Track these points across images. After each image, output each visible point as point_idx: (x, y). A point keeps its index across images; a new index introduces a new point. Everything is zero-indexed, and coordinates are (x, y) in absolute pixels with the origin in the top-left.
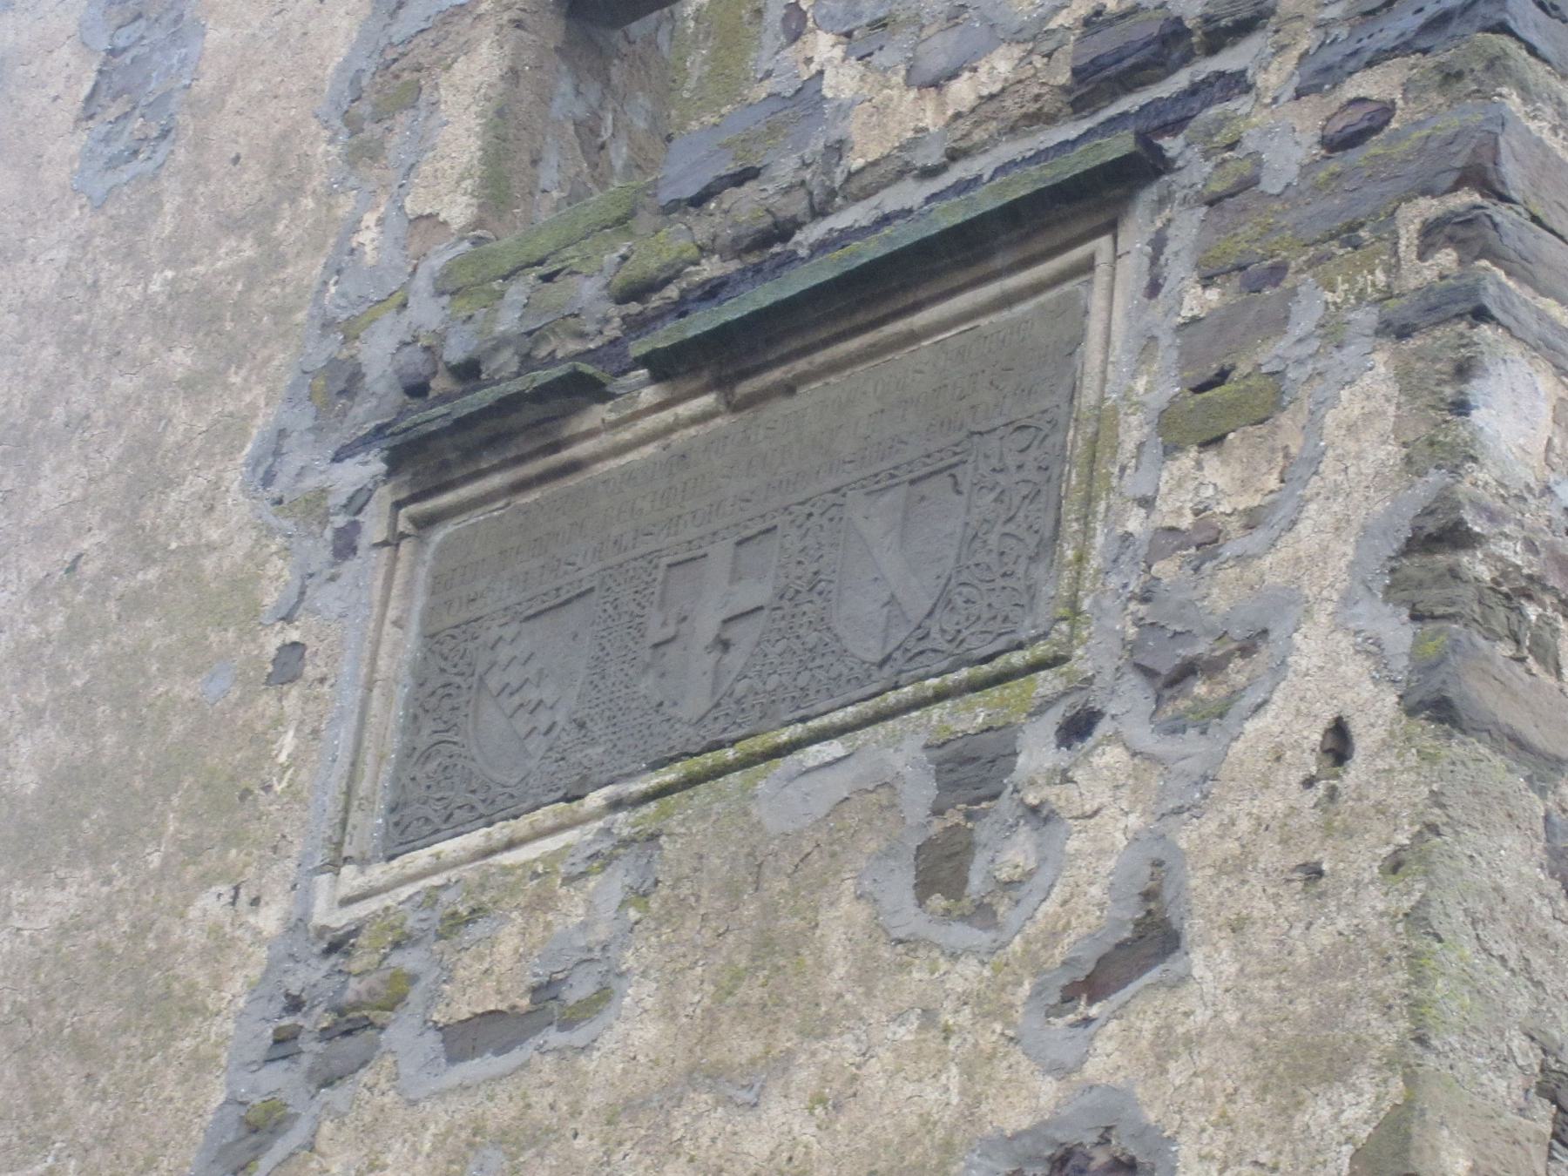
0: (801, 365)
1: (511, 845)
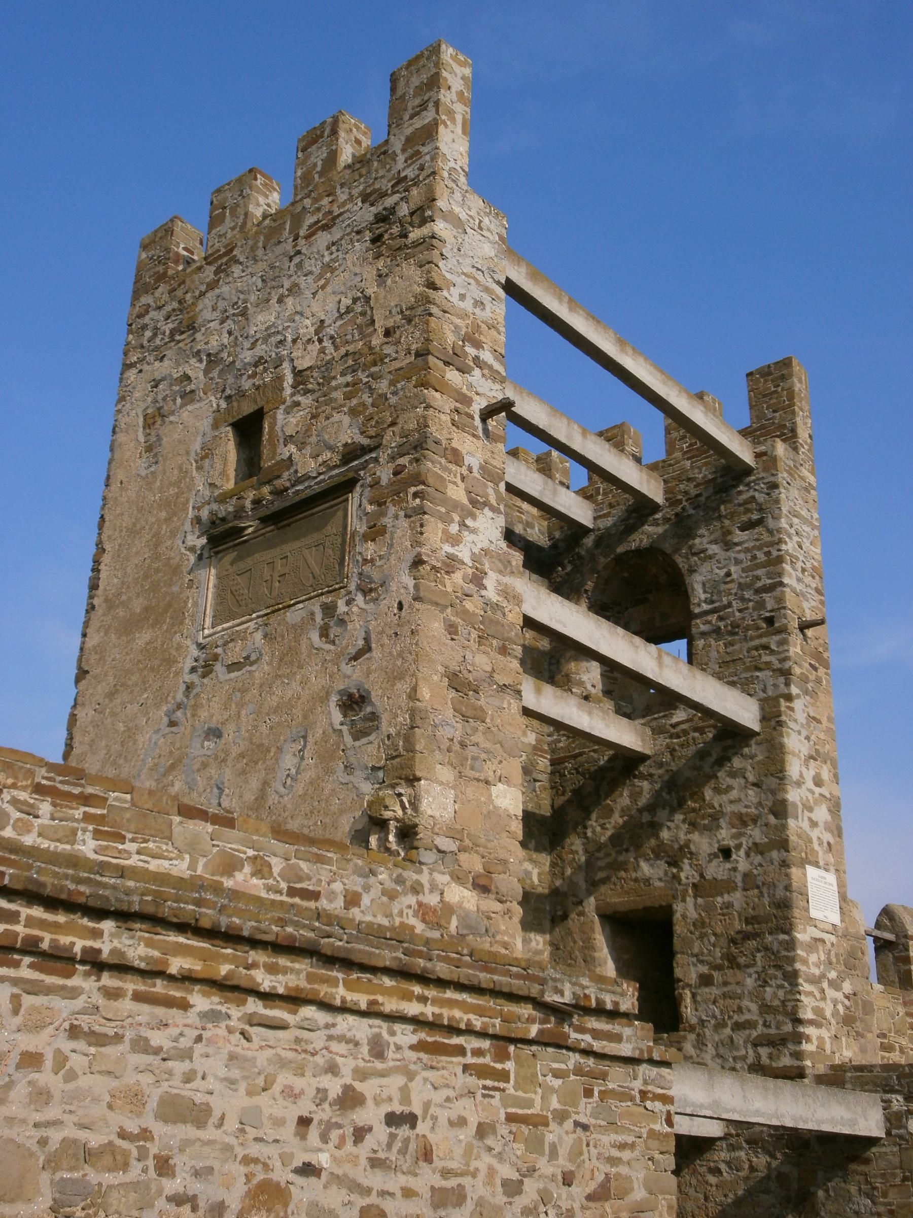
0: (291, 520)
1: (238, 625)
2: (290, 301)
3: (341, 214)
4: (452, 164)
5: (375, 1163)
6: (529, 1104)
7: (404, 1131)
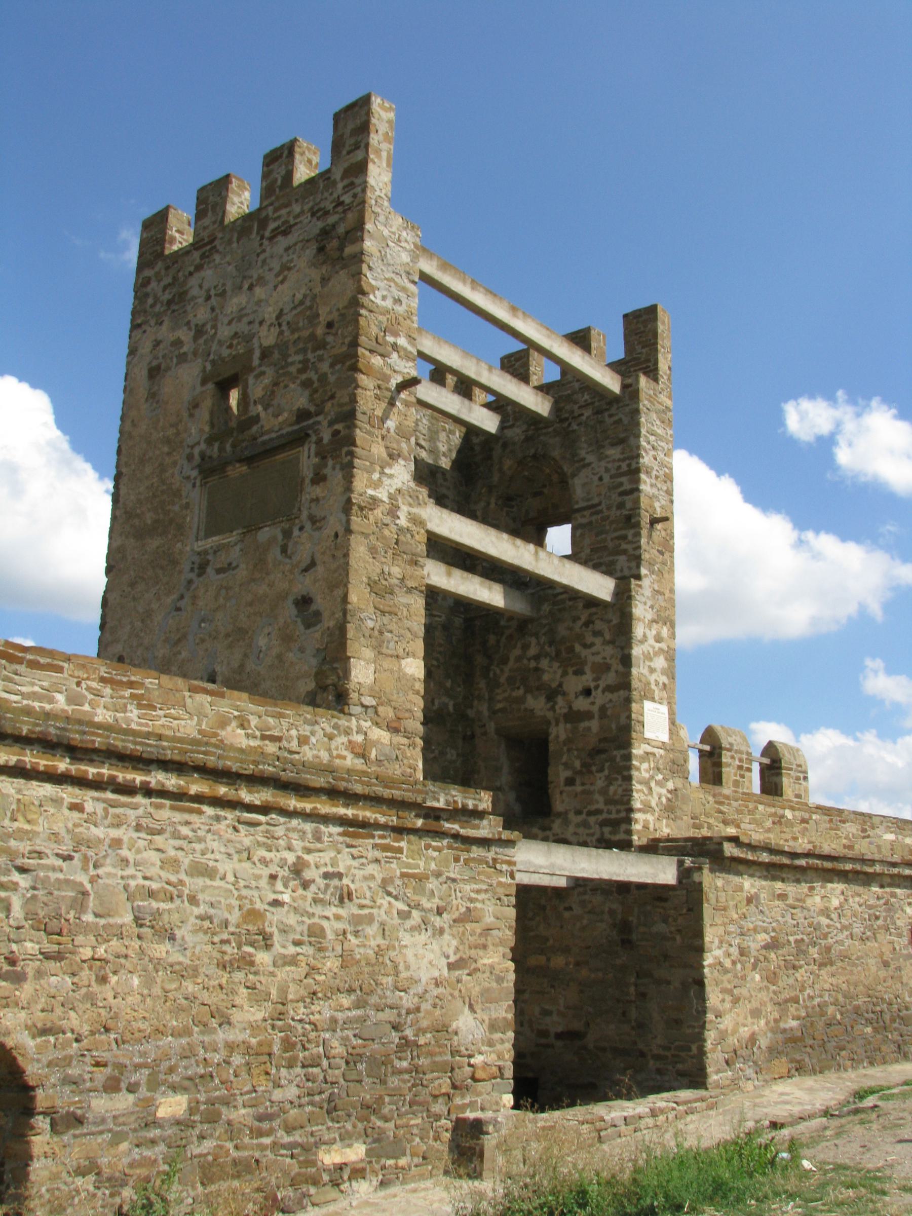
2: (258, 290)
3: (296, 224)
4: (377, 193)
5: (315, 901)
6: (418, 867)
7: (335, 882)
